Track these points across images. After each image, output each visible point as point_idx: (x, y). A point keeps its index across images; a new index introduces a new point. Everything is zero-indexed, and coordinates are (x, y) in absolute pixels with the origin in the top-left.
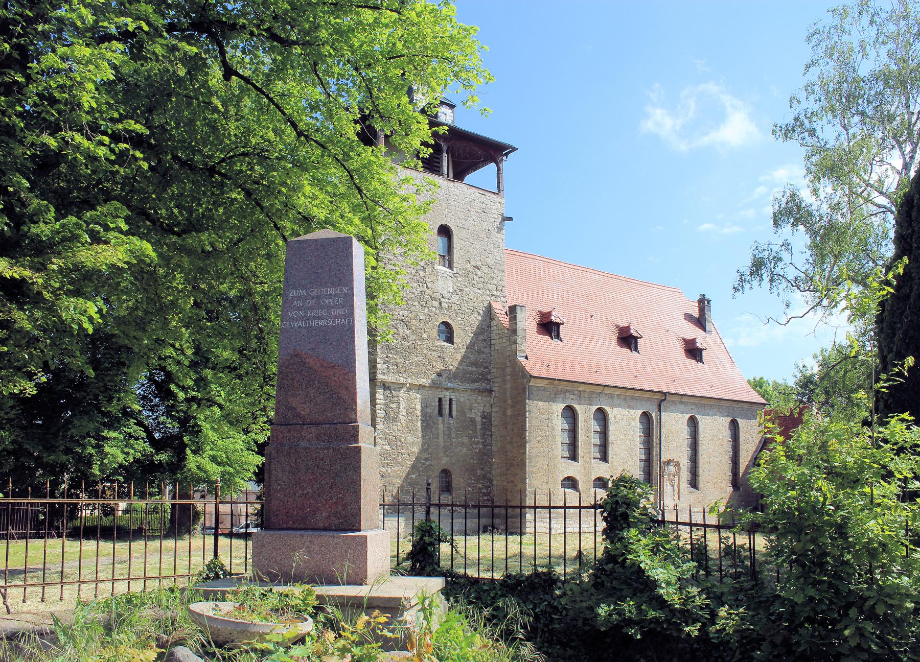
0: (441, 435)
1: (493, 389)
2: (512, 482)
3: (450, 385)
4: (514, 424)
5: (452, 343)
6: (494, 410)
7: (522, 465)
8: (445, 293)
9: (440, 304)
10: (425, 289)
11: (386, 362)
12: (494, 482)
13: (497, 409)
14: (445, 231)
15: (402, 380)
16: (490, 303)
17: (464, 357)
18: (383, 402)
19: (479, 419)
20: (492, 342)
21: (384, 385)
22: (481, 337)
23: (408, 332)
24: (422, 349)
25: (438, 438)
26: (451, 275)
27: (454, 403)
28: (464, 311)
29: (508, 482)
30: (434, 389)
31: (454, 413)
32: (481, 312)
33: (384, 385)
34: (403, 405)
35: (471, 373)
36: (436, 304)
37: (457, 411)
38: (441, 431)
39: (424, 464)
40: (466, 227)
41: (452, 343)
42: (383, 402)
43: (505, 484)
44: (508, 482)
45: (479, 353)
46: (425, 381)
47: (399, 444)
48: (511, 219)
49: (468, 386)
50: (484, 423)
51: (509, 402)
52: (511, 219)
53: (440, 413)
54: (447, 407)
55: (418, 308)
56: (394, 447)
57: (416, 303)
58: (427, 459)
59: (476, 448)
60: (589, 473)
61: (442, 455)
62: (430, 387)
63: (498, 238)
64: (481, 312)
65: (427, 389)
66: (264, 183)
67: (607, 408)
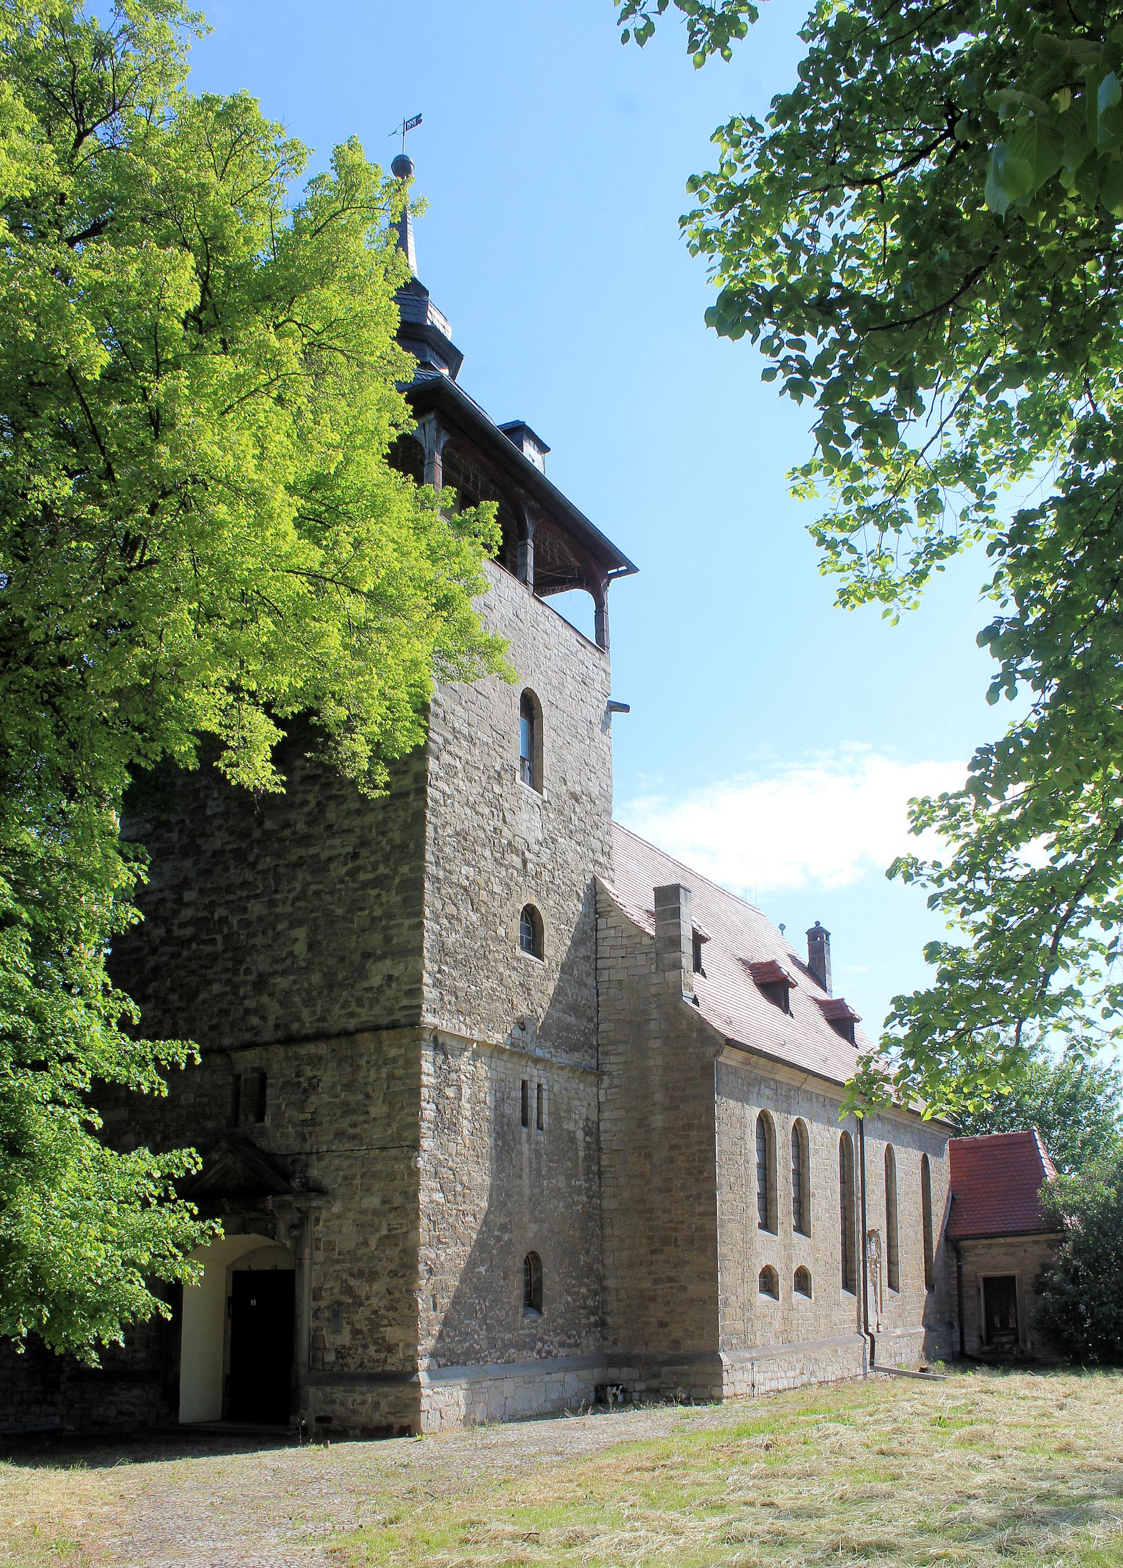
0: (526, 1171)
1: (606, 1068)
2: (670, 1279)
3: (539, 1053)
4: (674, 1147)
5: (540, 955)
6: (606, 1115)
7: (712, 1239)
8: (532, 841)
9: (525, 862)
10: (500, 824)
11: (438, 983)
12: (610, 1283)
13: (617, 1114)
14: (529, 705)
15: (464, 1032)
16: (594, 879)
17: (559, 990)
18: (434, 1081)
19: (580, 1135)
20: (600, 964)
21: (435, 1039)
22: (583, 952)
23: (474, 917)
24: (496, 961)
25: (520, 1177)
26: (540, 803)
27: (545, 1095)
28: (559, 887)
29: (656, 1282)
30: (515, 1060)
31: (545, 1118)
32: (582, 895)
33: (435, 1039)
34: (466, 1092)
35: (569, 1028)
36: (517, 861)
37: (550, 1114)
38: (525, 1161)
39: (499, 1239)
40: (560, 705)
41: (540, 955)
42: (434, 1081)
43: (646, 1284)
44: (656, 1282)
45: (579, 985)
46: (498, 1038)
47: (459, 1188)
48: (625, 708)
49: (564, 1058)
50: (588, 1147)
51: (658, 1097)
52: (625, 708)
53: (525, 1122)
54: (535, 1105)
55: (489, 865)
56: (451, 1198)
57: (487, 853)
58: (503, 1228)
59: (578, 1203)
60: (790, 1258)
61: (527, 1218)
62: (512, 1053)
63: (603, 743)
64: (582, 895)
65: (505, 1057)
66: (930, 334)
67: (806, 1120)
